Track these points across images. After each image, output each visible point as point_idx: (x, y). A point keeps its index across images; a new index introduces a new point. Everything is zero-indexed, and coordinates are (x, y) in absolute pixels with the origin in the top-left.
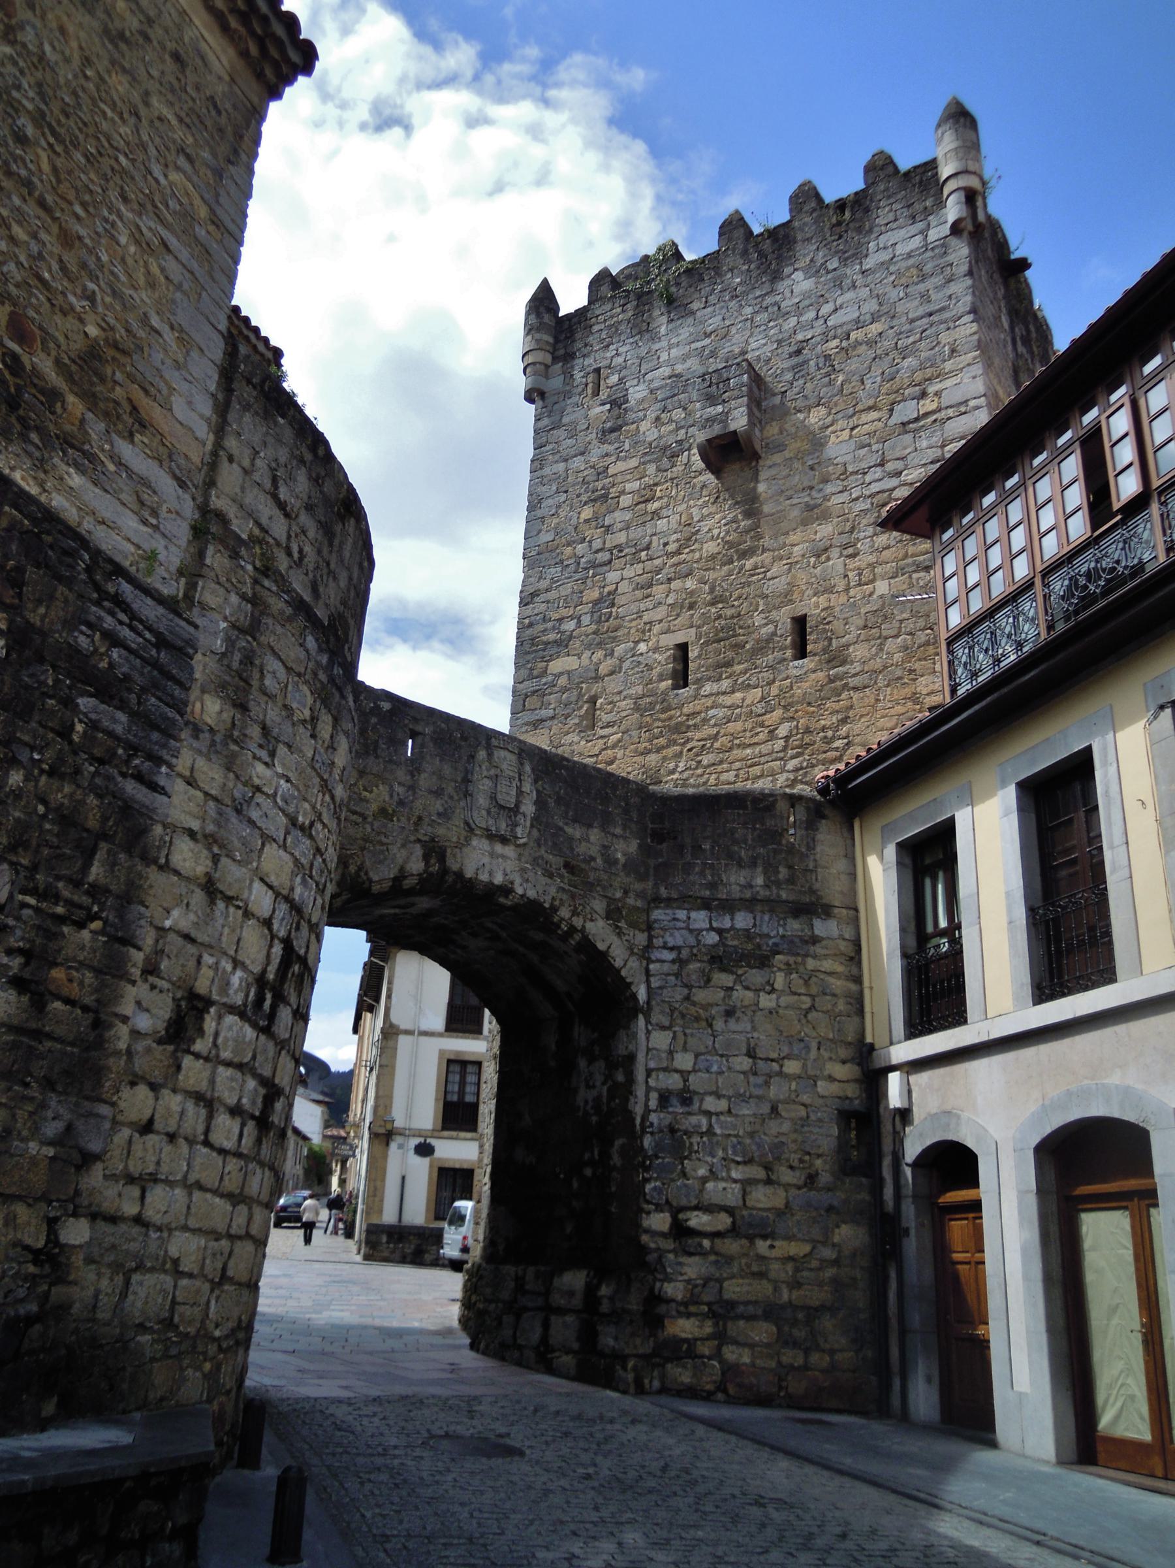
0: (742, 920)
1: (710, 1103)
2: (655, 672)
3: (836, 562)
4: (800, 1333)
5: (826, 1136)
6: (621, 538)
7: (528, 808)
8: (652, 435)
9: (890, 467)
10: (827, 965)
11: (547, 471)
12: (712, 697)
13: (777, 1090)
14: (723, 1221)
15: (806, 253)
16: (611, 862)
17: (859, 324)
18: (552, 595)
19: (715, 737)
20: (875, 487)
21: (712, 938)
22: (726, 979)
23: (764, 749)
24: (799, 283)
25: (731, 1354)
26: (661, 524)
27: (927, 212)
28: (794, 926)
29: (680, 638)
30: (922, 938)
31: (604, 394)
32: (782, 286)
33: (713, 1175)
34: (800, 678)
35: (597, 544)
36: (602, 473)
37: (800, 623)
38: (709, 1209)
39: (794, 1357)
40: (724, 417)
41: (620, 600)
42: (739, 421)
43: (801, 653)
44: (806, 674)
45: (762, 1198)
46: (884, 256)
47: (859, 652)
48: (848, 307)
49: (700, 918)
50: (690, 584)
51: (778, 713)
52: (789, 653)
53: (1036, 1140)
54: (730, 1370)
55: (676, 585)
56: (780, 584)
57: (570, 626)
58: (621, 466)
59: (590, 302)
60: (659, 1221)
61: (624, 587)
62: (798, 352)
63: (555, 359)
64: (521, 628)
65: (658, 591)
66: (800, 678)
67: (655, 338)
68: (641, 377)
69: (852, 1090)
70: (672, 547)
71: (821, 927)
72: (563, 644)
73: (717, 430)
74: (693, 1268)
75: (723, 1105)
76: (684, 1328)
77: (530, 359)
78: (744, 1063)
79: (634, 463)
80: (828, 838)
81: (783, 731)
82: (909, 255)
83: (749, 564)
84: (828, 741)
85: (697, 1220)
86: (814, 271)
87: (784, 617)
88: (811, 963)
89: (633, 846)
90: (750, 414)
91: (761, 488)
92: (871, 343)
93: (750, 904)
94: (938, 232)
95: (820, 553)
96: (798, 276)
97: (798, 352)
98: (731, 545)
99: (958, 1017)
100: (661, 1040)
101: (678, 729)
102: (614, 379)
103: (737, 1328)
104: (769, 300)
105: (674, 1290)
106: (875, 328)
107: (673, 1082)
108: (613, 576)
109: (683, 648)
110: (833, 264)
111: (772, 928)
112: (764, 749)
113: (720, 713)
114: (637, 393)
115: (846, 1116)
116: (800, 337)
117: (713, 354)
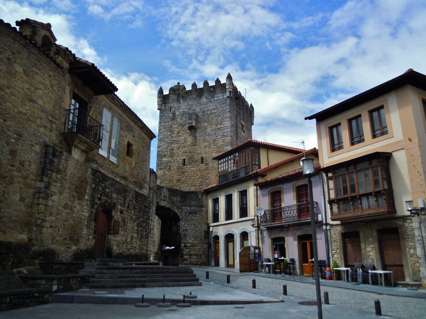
0: (193, 208)
1: (189, 231)
2: (180, 163)
3: (208, 149)
4: (199, 257)
5: (203, 234)
6: (175, 139)
7: (168, 196)
8: (180, 121)
9: (216, 135)
10: (204, 213)
11: (162, 124)
12: (189, 168)
13: (197, 229)
14: (191, 245)
15: (206, 94)
16: (177, 201)
17: (213, 109)
18: (163, 147)
19: (189, 175)
20: (214, 138)
21: (190, 210)
22: (191, 216)
23: (196, 177)
24: (204, 100)
25: (191, 260)
27: (224, 92)
28: (200, 209)
29: (184, 158)
30: (215, 211)
31: (172, 112)
33: (189, 239)
34: (202, 167)
35: (171, 139)
36: (171, 127)
37: (202, 158)
38: (189, 243)
39: (199, 260)
40: (192, 123)
41: (174, 150)
42: (194, 124)
43: (202, 163)
44: (203, 166)
46: (217, 98)
47: (210, 164)
48: (211, 106)
49: (188, 208)
50: (186, 149)
51: (198, 172)
54: (191, 261)
55: (183, 149)
56: (199, 151)
57: (166, 153)
58: (174, 126)
59: (169, 93)
60: (183, 245)
61: (175, 148)
62: (204, 112)
63: (163, 103)
64: (158, 152)
65: (181, 149)
66: (202, 167)
67: (180, 103)
68: (178, 110)
69: (206, 229)
70: (183, 142)
71: (203, 209)
72: (165, 156)
73: (190, 125)
74: (187, 250)
75: (191, 231)
76: (186, 257)
77: (159, 103)
78: (193, 226)
79: (177, 126)
80: (204, 197)
81: (199, 175)
82: (221, 99)
83: (195, 147)
84: (205, 177)
85: (188, 245)
86: (207, 98)
87: (200, 157)
88: (202, 213)
89: (180, 199)
90: (196, 122)
91: (197, 135)
92: (214, 113)
93: (194, 206)
94: (225, 97)
95: (206, 147)
96: (204, 98)
97: (204, 112)
98: (192, 143)
99: (218, 221)
100: (183, 223)
101: (184, 172)
102: (173, 109)
103: (192, 257)
104: (199, 101)
105: (185, 253)
106: (215, 111)
107: (185, 228)
108: (173, 145)
109: (184, 159)
110: (210, 98)
111: (197, 209)
112: (196, 177)
113: (190, 171)
114: (177, 113)
115: (205, 232)
117: (190, 109)
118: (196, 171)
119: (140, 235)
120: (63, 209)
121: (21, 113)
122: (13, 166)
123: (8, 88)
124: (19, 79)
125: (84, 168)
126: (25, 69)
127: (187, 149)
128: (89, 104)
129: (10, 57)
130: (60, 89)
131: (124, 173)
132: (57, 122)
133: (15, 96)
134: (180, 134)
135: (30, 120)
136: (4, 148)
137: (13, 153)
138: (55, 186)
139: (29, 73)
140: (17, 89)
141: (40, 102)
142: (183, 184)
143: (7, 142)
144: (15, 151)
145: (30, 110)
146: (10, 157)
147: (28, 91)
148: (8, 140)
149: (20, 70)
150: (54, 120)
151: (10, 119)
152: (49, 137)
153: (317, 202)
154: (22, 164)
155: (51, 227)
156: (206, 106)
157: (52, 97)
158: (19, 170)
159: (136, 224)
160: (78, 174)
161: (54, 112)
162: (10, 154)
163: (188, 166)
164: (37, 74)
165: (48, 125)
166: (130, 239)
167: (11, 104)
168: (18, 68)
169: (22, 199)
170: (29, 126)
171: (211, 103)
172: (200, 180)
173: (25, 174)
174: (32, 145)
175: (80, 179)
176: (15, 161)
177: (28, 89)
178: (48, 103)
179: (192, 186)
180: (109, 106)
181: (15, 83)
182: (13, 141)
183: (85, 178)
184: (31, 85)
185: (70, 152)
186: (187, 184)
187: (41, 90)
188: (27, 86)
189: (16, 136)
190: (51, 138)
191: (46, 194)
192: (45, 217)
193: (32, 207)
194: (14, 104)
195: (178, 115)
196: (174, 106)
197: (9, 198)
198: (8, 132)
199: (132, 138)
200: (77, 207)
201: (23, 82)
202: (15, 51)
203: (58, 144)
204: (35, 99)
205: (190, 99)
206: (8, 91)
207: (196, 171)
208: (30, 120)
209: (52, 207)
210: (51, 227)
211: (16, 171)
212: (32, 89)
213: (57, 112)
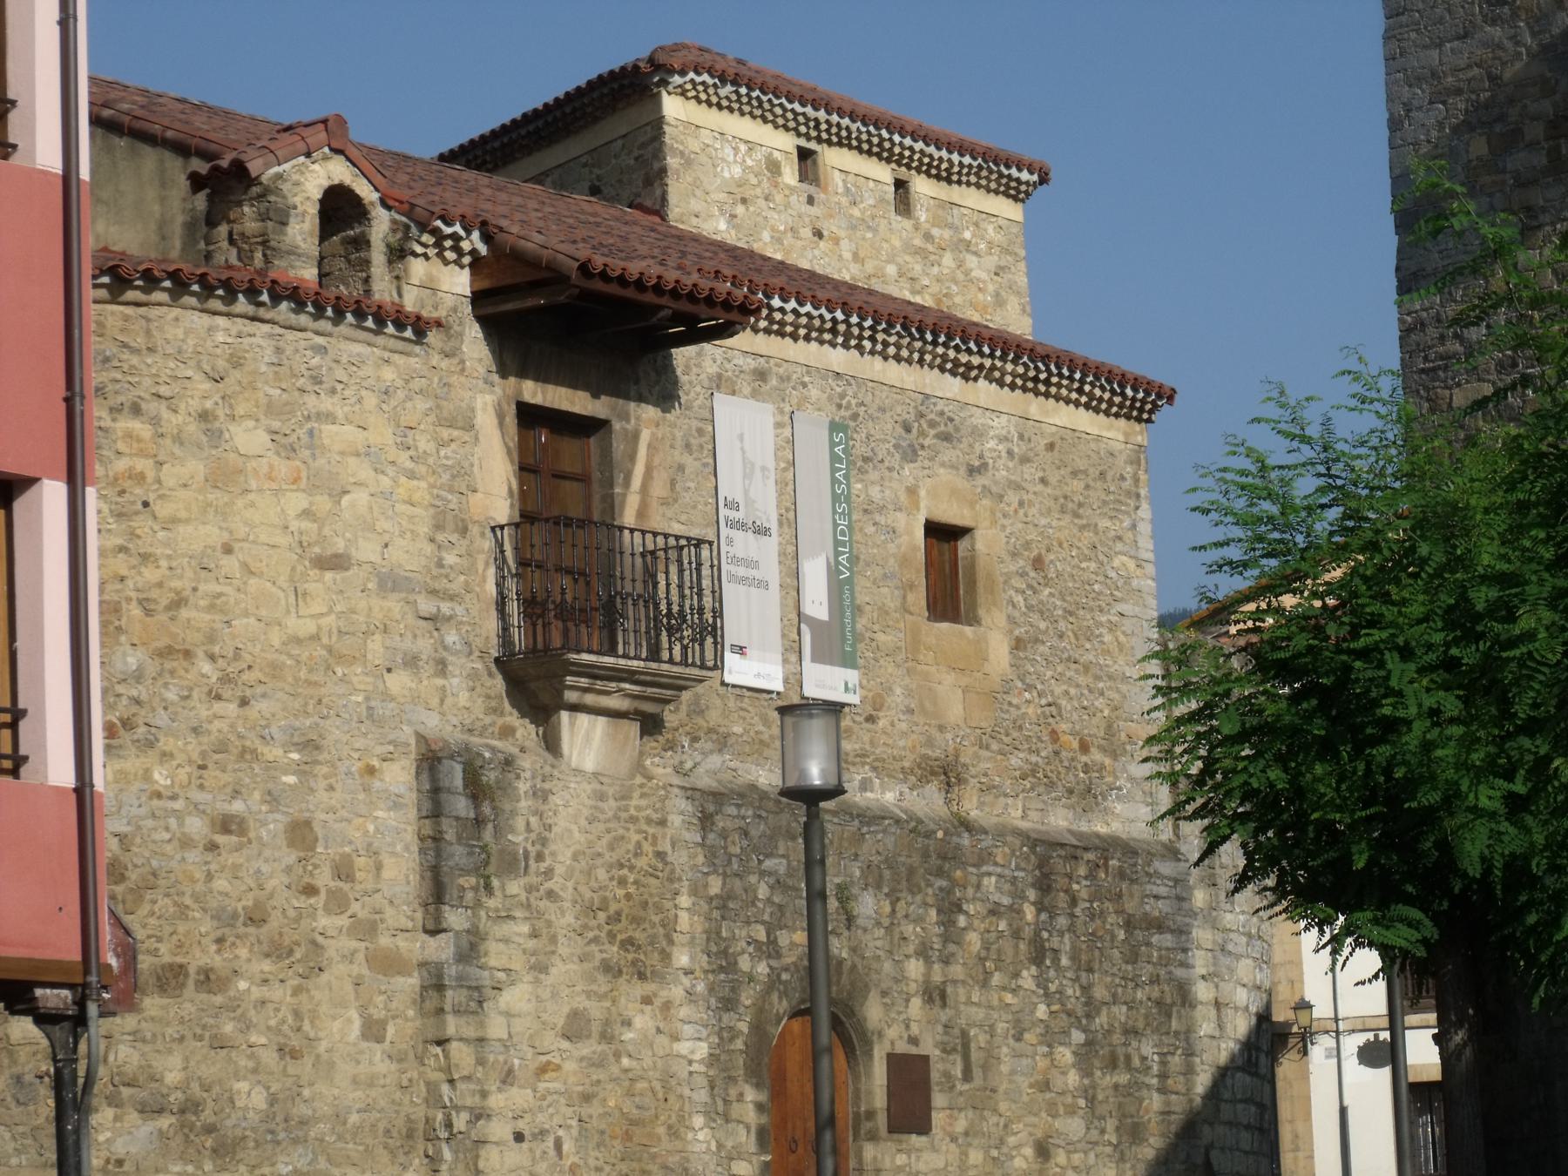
119: (1111, 1124)
120: (565, 1044)
121: (298, 641)
122: (310, 890)
123: (228, 550)
124: (260, 491)
125: (643, 802)
126: (276, 425)
128: (617, 426)
129: (209, 404)
130: (446, 433)
131: (930, 742)
132: (459, 610)
133: (261, 575)
135: (340, 658)
136: (264, 824)
137: (301, 834)
138: (506, 941)
139: (293, 438)
140: (263, 538)
141: (367, 550)
143: (269, 793)
144: (308, 823)
145: (331, 611)
146: (291, 857)
147: (306, 525)
148: (270, 786)
150: (446, 608)
151: (259, 690)
152: (435, 702)
154: (344, 871)
155: (519, 1137)
157: (416, 497)
158: (338, 903)
159: (1065, 1055)
160: (611, 848)
161: (440, 565)
162: (292, 844)
164: (330, 418)
165: (424, 646)
166: (1029, 1151)
167: (252, 620)
168: (249, 438)
169: (373, 1030)
170: (341, 689)
174: (371, 771)
175: (632, 868)
176: (316, 866)
178: (402, 534)
180: (751, 363)
182: (291, 779)
183: (660, 855)
184: (312, 489)
185: (552, 744)
188: (296, 502)
189: (295, 756)
190: (449, 701)
191: (469, 988)
192: (484, 1094)
193: (421, 1060)
194: (263, 612)
197: (321, 1034)
198: (266, 750)
199: (962, 483)
200: (638, 1022)
202: (221, 364)
203: (488, 720)
204: (340, 546)
206: (230, 564)
208: (340, 658)
209: (507, 1044)
210: (519, 1137)
211: (328, 911)
213: (450, 559)
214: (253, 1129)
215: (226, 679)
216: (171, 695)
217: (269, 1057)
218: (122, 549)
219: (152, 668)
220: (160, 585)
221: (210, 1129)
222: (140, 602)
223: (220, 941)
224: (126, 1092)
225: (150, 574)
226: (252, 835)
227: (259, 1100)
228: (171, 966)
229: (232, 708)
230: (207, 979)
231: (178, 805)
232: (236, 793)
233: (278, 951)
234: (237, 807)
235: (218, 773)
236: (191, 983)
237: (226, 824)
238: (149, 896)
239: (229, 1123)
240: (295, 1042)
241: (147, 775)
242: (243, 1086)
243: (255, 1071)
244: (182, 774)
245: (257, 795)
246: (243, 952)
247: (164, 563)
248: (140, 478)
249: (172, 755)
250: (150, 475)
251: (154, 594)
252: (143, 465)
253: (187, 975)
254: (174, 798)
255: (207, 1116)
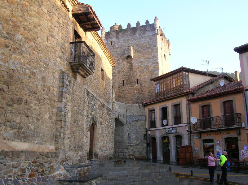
1: (133, 134)
14: (134, 144)
15: (138, 32)
17: (144, 43)
20: (146, 65)
24: (137, 36)
26: (121, 64)
29: (123, 79)
31: (112, 45)
32: (135, 35)
37: (137, 79)
45: (137, 142)
48: (143, 40)
52: (136, 83)
53: (161, 137)
61: (116, 72)
68: (117, 44)
73: (128, 55)
74: (132, 148)
79: (117, 55)
85: (132, 144)
91: (133, 62)
94: (153, 34)
96: (137, 35)
101: (123, 90)
102: (114, 43)
114: (117, 46)
115: (145, 135)
116: (138, 43)
118: (132, 89)
121: (47, 46)
122: (44, 90)
123: (39, 26)
127: (125, 72)
133: (43, 33)
134: (119, 62)
137: (44, 79)
141: (57, 37)
142: (123, 99)
145: (52, 44)
149: (45, 11)
150: (65, 52)
151: (40, 52)
152: (62, 66)
153: (241, 114)
154: (49, 89)
156: (139, 41)
163: (127, 86)
164: (55, 14)
167: (41, 39)
169: (50, 118)
170: (52, 57)
171: (143, 38)
172: (136, 96)
173: (51, 97)
174: (54, 73)
177: (50, 26)
179: (130, 101)
181: (43, 21)
185: (75, 78)
186: (126, 99)
187: (57, 27)
188: (50, 24)
189: (45, 66)
193: (56, 124)
195: (118, 47)
196: (114, 41)
201: (47, 21)
204: (54, 35)
205: (127, 35)
206: (39, 28)
207: (132, 89)
210: (68, 138)
212: (53, 26)
214: (31, 134)
215: (36, 47)
216: (26, 46)
217: (35, 120)
218: (21, 17)
219: (23, 40)
220: (27, 26)
221: (24, 133)
222: (23, 27)
223: (29, 95)
224: (8, 123)
225: (26, 23)
226: (36, 77)
227: (32, 128)
228: (20, 98)
229: (36, 53)
230: (26, 103)
231: (25, 67)
232: (35, 68)
233: (38, 100)
234: (35, 71)
235: (32, 63)
236: (23, 102)
237: (33, 74)
238: (17, 83)
239: (27, 132)
240: (39, 117)
241: (20, 59)
242: (30, 125)
243: (33, 122)
244: (27, 61)
245: (38, 70)
246: (33, 99)
247: (29, 22)
248: (27, 6)
249: (25, 57)
250: (29, 7)
251: (26, 27)
252: (27, 4)
253: (23, 101)
254: (24, 65)
255: (23, 130)
